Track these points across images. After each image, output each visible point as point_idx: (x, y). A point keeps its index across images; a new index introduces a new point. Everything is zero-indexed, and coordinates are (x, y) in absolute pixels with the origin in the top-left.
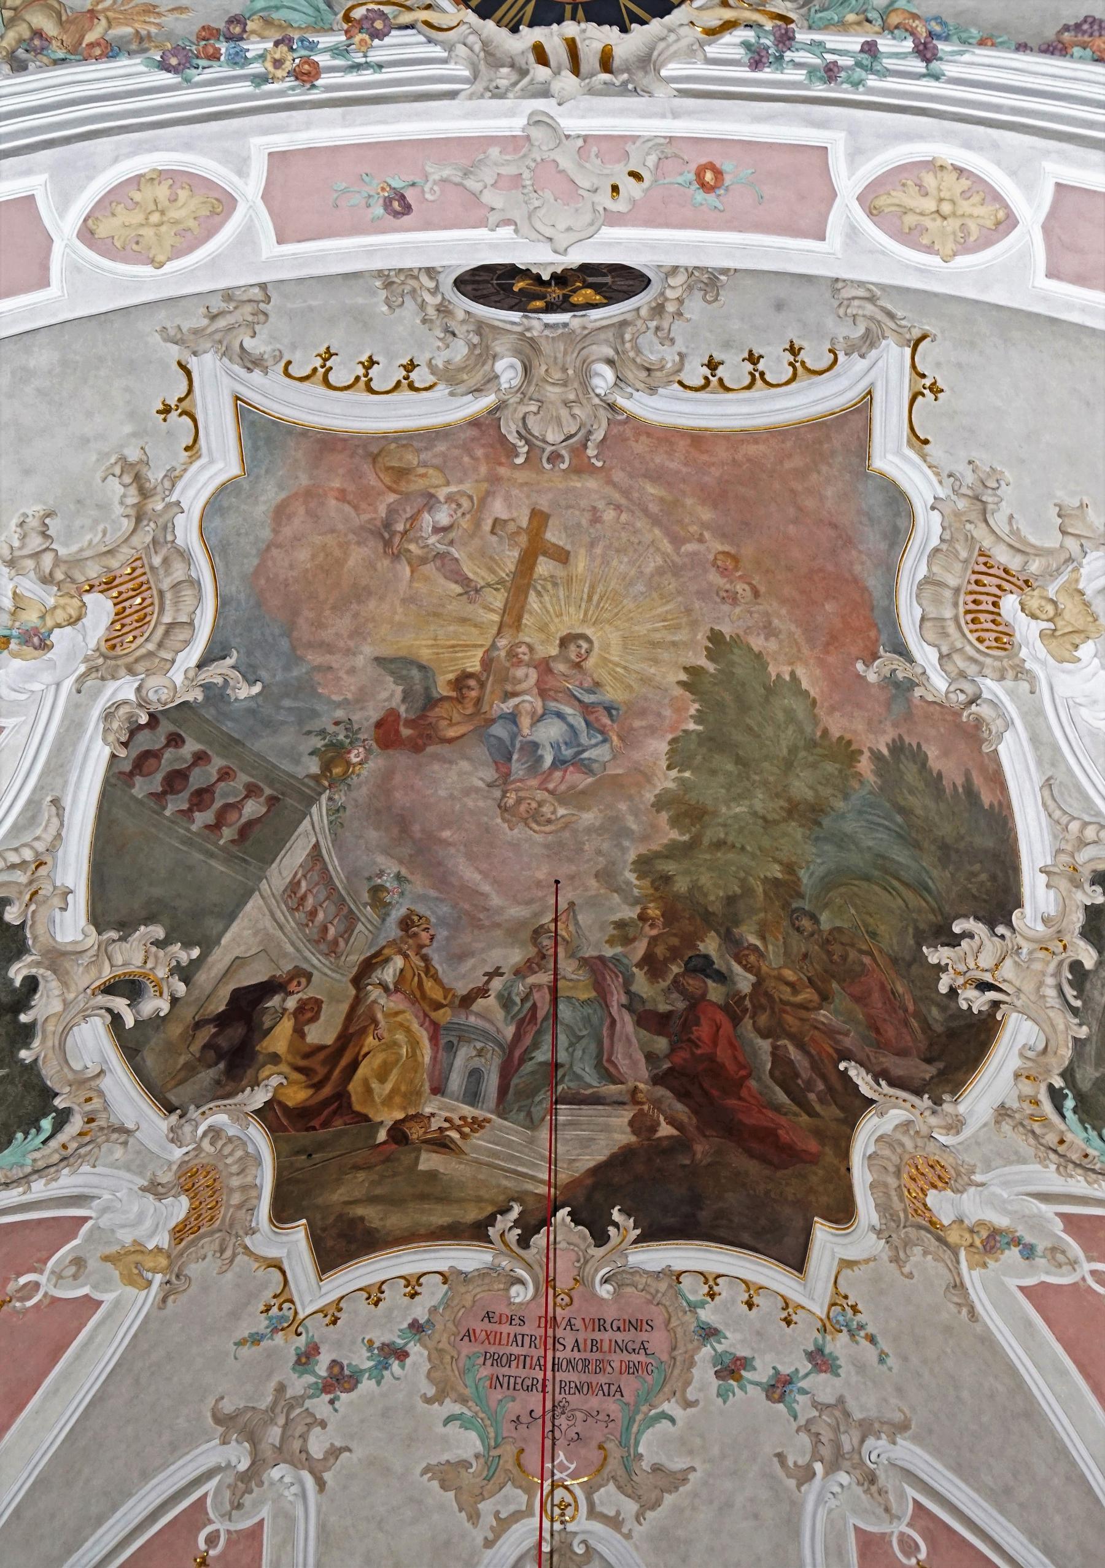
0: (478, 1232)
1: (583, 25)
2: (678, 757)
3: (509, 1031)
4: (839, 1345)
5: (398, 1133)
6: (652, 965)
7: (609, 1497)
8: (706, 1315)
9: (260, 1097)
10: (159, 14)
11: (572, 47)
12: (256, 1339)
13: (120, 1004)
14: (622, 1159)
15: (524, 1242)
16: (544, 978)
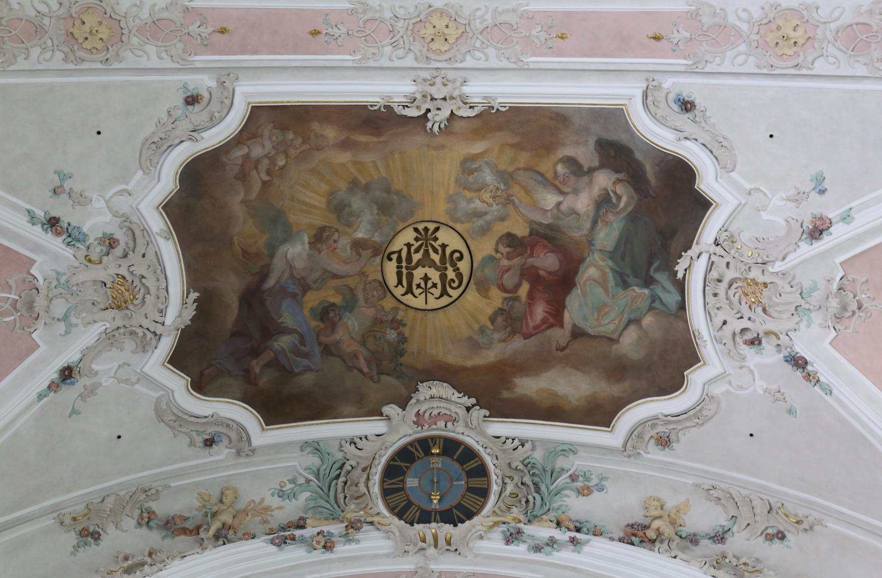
1: (439, 525)
10: (272, 510)
11: (435, 538)
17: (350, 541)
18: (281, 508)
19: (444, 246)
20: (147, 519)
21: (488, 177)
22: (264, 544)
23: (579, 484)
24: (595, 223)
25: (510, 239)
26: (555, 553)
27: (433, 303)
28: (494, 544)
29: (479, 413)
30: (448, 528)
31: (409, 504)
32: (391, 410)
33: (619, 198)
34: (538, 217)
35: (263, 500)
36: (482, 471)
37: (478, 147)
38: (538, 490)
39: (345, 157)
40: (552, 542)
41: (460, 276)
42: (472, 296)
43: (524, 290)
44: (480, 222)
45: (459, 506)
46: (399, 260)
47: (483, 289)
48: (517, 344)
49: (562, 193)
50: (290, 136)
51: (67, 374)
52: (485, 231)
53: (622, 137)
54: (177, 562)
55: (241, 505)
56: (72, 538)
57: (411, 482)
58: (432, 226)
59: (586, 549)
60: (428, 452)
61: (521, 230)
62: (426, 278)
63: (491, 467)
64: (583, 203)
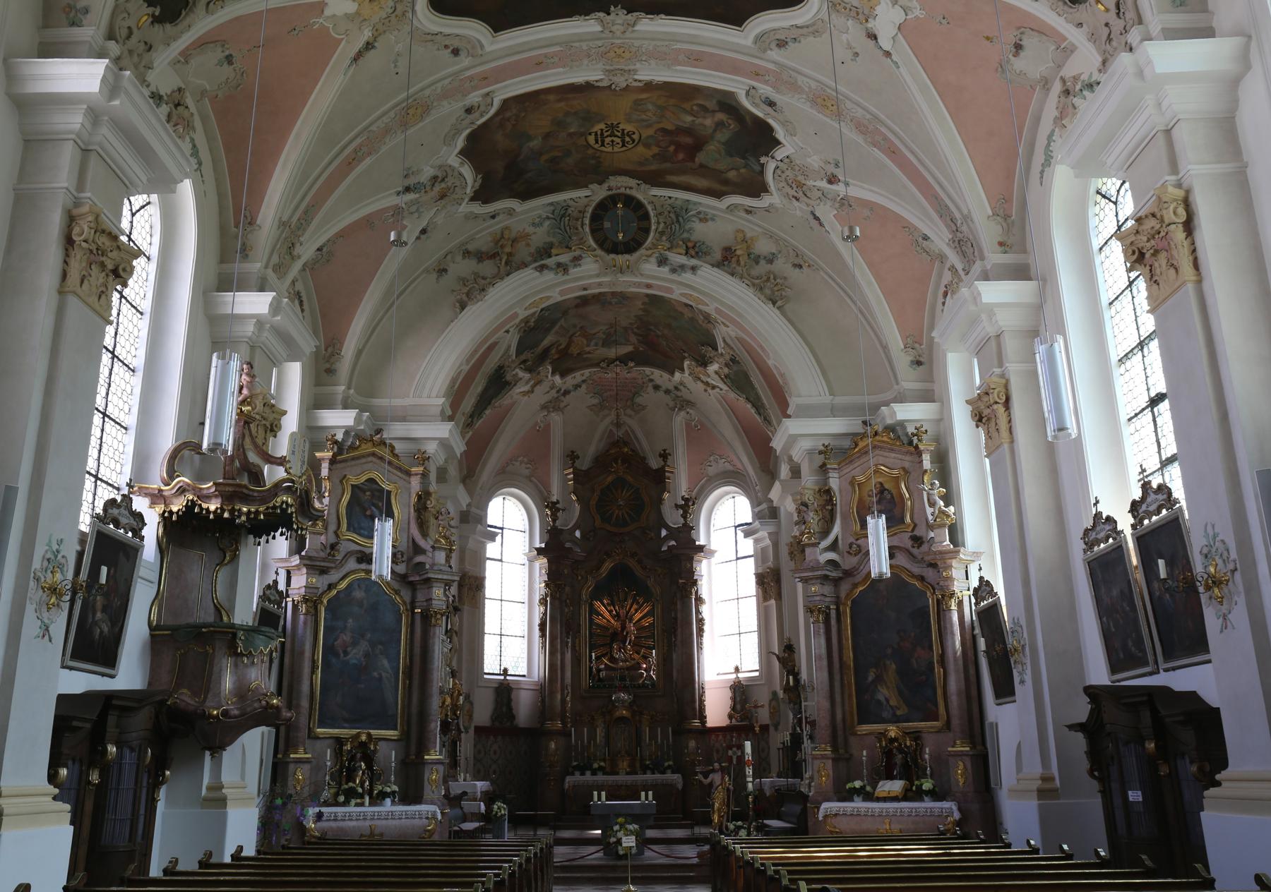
0: (597, 365)
2: (643, 304)
3: (604, 337)
4: (681, 387)
5: (578, 354)
6: (638, 328)
7: (629, 411)
8: (651, 377)
9: (549, 361)
12: (548, 392)
13: (522, 366)
14: (631, 353)
15: (608, 366)
16: (613, 329)
17: (575, 266)
18: (535, 233)
19: (623, 130)
20: (467, 254)
21: (650, 107)
22: (532, 271)
23: (701, 216)
24: (715, 131)
25: (663, 130)
26: (683, 275)
27: (616, 149)
28: (650, 267)
29: (643, 186)
30: (627, 256)
31: (606, 238)
32: (594, 186)
33: (730, 125)
34: (681, 124)
35: (524, 229)
36: (646, 217)
37: (644, 96)
38: (678, 221)
39: (562, 104)
40: (682, 267)
41: (633, 141)
42: (640, 149)
43: (672, 148)
44: (645, 123)
45: (633, 239)
46: (596, 134)
47: (647, 146)
48: (668, 165)
49: (695, 116)
50: (527, 104)
51: (424, 231)
52: (649, 126)
53: (734, 104)
54: (491, 289)
55: (513, 235)
56: (435, 275)
57: (607, 225)
58: (615, 123)
59: (699, 272)
60: (615, 205)
61: (670, 127)
62: (613, 141)
63: (652, 214)
64: (708, 122)
